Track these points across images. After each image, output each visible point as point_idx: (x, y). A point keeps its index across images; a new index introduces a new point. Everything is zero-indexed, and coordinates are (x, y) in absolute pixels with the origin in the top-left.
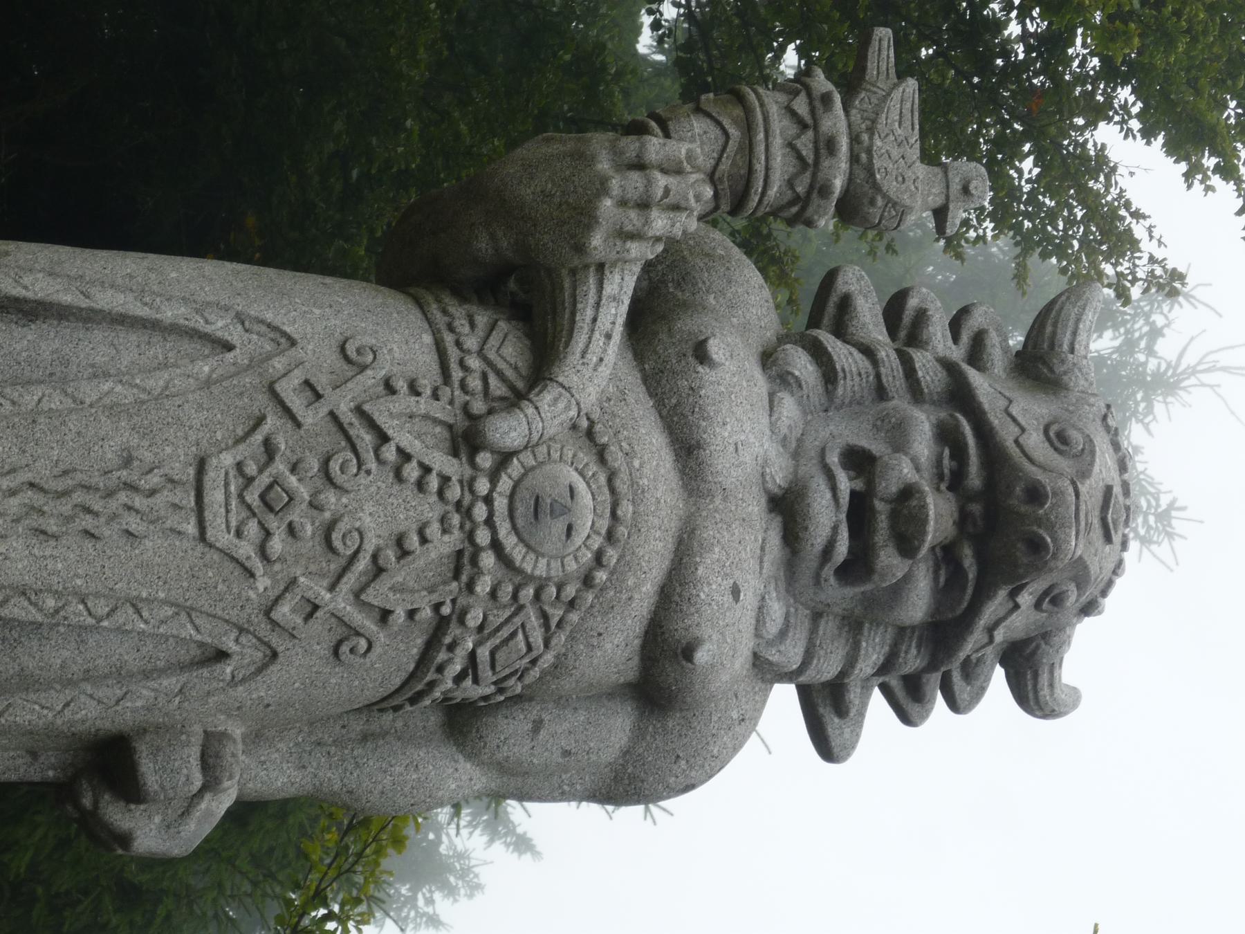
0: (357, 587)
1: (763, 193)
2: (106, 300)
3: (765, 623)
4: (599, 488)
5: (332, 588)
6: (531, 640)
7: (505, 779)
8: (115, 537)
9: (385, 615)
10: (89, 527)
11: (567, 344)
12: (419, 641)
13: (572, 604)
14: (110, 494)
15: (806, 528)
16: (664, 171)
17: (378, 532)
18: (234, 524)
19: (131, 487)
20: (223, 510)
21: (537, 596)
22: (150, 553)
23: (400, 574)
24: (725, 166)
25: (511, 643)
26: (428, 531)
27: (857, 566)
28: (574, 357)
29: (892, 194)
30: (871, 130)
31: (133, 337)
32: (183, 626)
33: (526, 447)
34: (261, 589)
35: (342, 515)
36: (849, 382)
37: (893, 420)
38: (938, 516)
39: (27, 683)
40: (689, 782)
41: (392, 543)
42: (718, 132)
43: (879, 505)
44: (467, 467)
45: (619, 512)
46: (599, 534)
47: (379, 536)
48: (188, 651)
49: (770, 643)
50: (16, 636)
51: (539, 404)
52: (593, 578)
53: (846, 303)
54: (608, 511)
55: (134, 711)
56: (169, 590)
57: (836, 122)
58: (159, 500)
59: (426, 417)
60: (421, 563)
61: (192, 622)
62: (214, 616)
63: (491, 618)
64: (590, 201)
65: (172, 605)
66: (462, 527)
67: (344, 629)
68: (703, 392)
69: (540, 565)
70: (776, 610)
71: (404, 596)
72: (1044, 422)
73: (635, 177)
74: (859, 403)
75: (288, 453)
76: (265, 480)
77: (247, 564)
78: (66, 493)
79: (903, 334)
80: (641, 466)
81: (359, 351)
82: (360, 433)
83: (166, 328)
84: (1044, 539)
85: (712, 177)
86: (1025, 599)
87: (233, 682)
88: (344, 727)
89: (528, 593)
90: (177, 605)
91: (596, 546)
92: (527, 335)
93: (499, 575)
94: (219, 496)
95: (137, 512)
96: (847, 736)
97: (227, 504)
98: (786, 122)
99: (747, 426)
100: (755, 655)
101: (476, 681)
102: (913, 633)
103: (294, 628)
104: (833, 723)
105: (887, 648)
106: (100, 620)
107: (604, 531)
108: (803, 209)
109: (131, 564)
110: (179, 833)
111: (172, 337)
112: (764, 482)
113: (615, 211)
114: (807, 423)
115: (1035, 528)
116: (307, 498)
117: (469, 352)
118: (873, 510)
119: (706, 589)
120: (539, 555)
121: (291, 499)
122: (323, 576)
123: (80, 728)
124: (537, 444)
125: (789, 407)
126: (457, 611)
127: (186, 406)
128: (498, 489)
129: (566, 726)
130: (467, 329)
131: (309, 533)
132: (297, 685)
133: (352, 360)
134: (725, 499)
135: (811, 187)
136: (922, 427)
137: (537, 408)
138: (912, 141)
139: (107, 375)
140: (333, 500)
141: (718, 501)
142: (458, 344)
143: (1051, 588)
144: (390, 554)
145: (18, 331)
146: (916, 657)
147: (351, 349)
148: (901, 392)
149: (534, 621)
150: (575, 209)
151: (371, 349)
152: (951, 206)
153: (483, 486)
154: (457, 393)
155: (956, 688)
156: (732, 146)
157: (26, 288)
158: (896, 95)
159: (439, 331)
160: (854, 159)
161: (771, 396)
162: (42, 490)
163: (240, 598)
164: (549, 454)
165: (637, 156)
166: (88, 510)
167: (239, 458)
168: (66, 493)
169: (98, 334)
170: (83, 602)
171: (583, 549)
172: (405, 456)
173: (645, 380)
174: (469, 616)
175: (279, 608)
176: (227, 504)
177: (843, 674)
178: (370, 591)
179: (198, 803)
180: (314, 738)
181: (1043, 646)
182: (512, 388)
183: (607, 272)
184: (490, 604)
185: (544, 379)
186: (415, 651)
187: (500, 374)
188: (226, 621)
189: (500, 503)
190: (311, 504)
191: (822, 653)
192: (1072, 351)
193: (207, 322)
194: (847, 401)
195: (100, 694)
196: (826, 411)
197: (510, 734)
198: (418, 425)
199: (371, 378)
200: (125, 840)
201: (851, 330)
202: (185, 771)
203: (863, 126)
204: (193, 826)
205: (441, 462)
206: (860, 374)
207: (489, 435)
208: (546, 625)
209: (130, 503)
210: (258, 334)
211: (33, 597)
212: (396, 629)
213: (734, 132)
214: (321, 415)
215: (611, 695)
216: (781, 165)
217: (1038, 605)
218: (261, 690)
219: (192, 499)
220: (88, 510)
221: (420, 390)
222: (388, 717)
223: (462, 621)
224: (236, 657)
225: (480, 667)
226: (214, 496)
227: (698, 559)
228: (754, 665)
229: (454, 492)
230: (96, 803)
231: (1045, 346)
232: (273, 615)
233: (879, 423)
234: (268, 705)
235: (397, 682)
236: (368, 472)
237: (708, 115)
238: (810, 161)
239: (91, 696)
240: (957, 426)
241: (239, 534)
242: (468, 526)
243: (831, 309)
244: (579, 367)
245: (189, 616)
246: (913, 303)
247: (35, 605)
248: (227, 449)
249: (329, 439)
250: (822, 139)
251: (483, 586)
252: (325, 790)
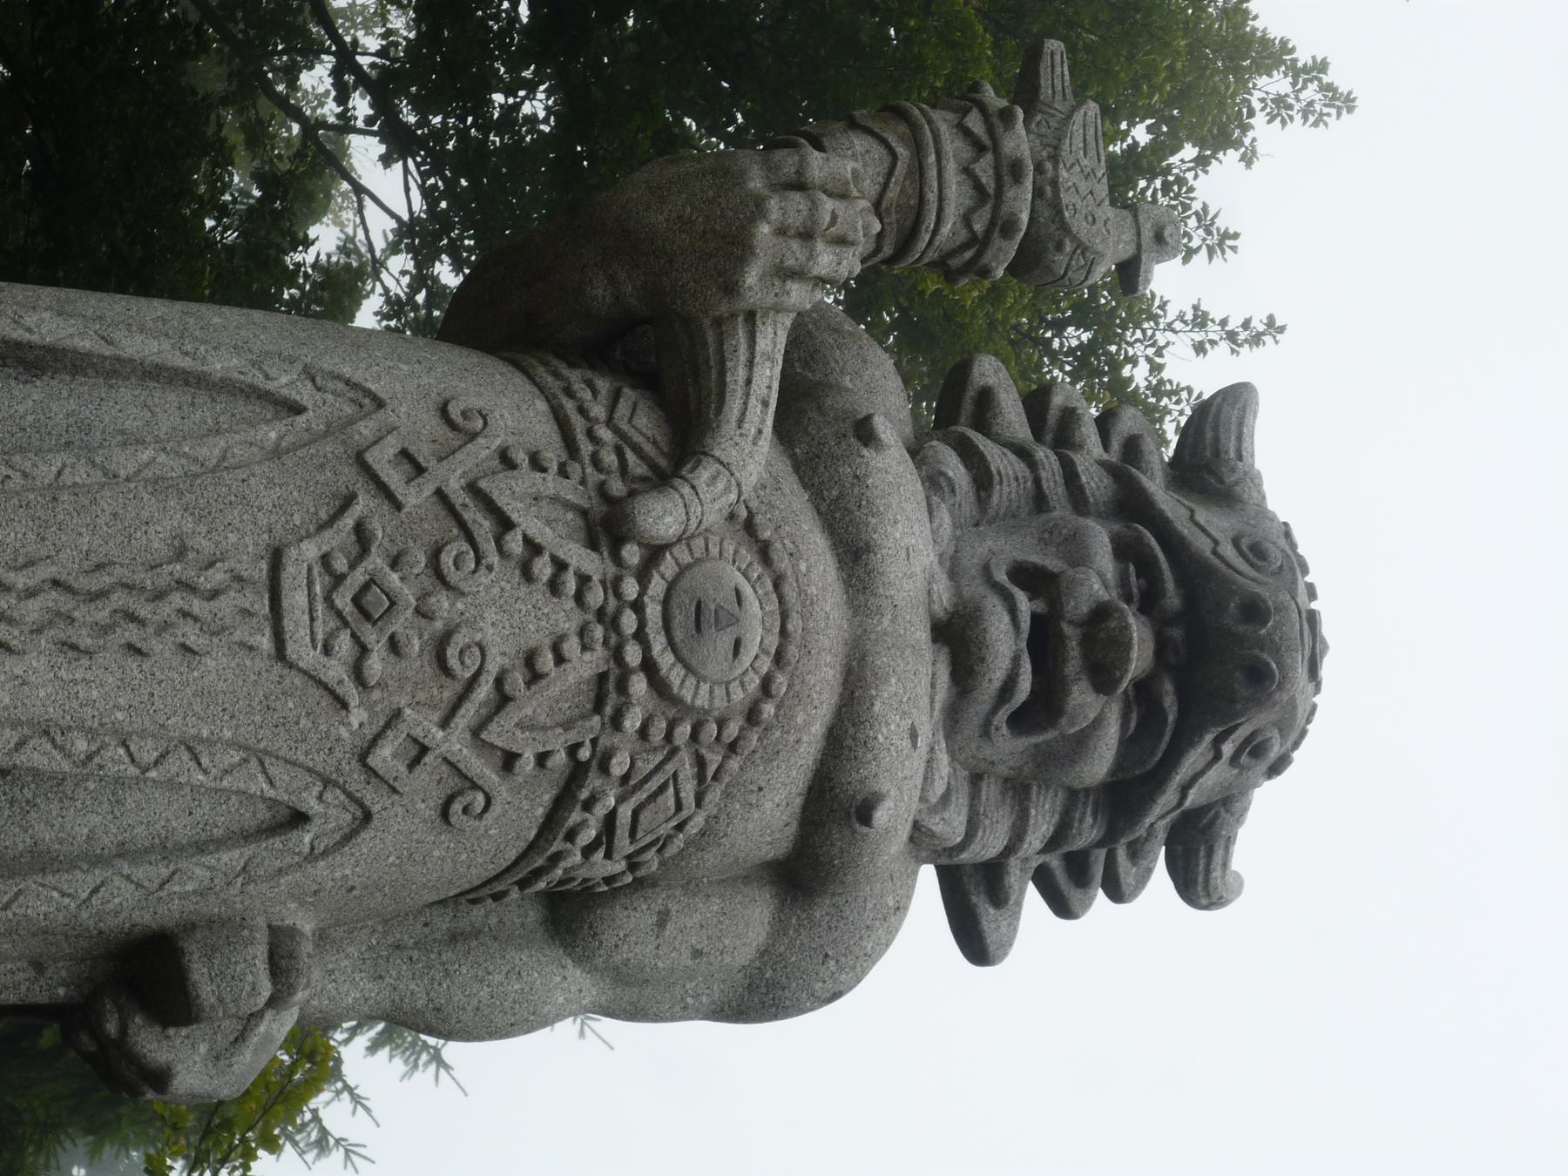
0: (474, 722)
1: (935, 232)
2: (135, 346)
3: (933, 781)
4: (766, 594)
5: (445, 723)
6: (683, 795)
7: (618, 990)
8: (168, 654)
9: (509, 761)
10: (135, 640)
11: (719, 410)
12: (547, 797)
13: (733, 748)
14: (159, 596)
15: (983, 660)
16: (830, 195)
17: (504, 648)
18: (320, 637)
19: (188, 587)
20: (306, 617)
21: (694, 737)
22: (213, 676)
23: (530, 705)
24: (892, 194)
25: (660, 799)
26: (565, 646)
27: (1042, 709)
28: (729, 427)
29: (1082, 236)
30: (1055, 159)
31: (172, 397)
32: (253, 777)
33: (679, 540)
34: (356, 725)
35: (458, 625)
36: (1006, 489)
37: (1065, 531)
38: (1140, 638)
39: (42, 862)
40: (837, 989)
41: (519, 663)
42: (883, 150)
43: (1068, 629)
44: (609, 562)
45: (790, 627)
46: (768, 653)
47: (504, 654)
48: (254, 813)
49: (933, 810)
50: (30, 796)
51: (695, 482)
52: (760, 712)
53: (986, 398)
54: (778, 623)
55: (184, 896)
56: (237, 726)
57: (1019, 141)
58: (225, 606)
59: (554, 499)
60: (555, 690)
61: (264, 772)
62: (294, 764)
63: (639, 764)
64: (744, 228)
65: (241, 747)
66: (605, 642)
67: (457, 780)
68: (870, 482)
69: (701, 692)
71: (534, 735)
72: (1231, 534)
73: (796, 196)
74: (1014, 516)
75: (386, 543)
76: (359, 577)
77: (340, 691)
78: (101, 595)
79: (1049, 437)
80: (808, 570)
81: (464, 414)
82: (477, 518)
83: (214, 385)
84: (1268, 664)
85: (877, 207)
86: (1228, 749)
87: (312, 856)
88: (426, 925)
89: (684, 730)
90: (247, 748)
91: (765, 670)
92: (659, 406)
93: (650, 707)
94: (301, 599)
95: (196, 619)
96: (1003, 929)
97: (311, 611)
98: (959, 143)
99: (916, 527)
100: (916, 826)
101: (608, 855)
102: (1087, 796)
103: (396, 779)
104: (988, 916)
105: (1057, 817)
106: (145, 770)
107: (773, 651)
108: (979, 254)
109: (188, 690)
110: (231, 1066)
111: (223, 397)
112: (931, 602)
113: (775, 240)
114: (958, 539)
115: (1257, 651)
116: (414, 603)
117: (597, 421)
118: (1061, 638)
119: (884, 730)
120: (700, 679)
121: (393, 603)
122: (434, 707)
123: (112, 922)
124: (692, 536)
126: (598, 755)
127: (253, 481)
128: (650, 592)
129: (697, 918)
130: (588, 395)
131: (417, 648)
132: (391, 859)
133: (457, 427)
134: (893, 621)
135: (992, 224)
136: (1100, 539)
137: (693, 487)
138: (1099, 175)
139: (141, 442)
140: (446, 605)
141: (886, 622)
142: (582, 411)
143: (1254, 734)
144: (518, 678)
145: (18, 390)
146: (1092, 827)
147: (455, 411)
148: (1063, 501)
149: (687, 770)
150: (724, 237)
151: (480, 413)
152: (1144, 258)
153: (631, 589)
154: (589, 470)
155: (1121, 869)
156: (901, 168)
157: (29, 330)
158: (1078, 117)
159: (555, 396)
160: (1038, 192)
161: (928, 498)
162: (70, 590)
163: (328, 737)
164: (707, 549)
165: (797, 172)
166: (132, 617)
167: (325, 548)
168: (101, 595)
170: (124, 744)
171: (751, 672)
172: (533, 548)
173: (797, 468)
174: (614, 761)
175: (378, 751)
176: (311, 611)
177: (1009, 850)
178: (493, 727)
179: (256, 1026)
180: (390, 940)
181: (1223, 814)
182: (653, 466)
183: (759, 323)
184: (638, 746)
185: (695, 453)
186: (540, 811)
187: (637, 449)
188: (309, 770)
189: (653, 611)
190: (417, 611)
191: (987, 822)
192: (1240, 457)
193: (267, 377)
194: (1002, 512)
195: (139, 874)
196: (977, 525)
197: (630, 929)
198: (546, 508)
199: (483, 450)
200: (160, 1078)
201: (995, 429)
202: (250, 978)
203: (1044, 153)
204: (248, 1056)
205: (580, 557)
206: (1017, 479)
207: (640, 519)
208: (701, 777)
209: (186, 607)
210: (334, 393)
211: (58, 738)
212: (520, 779)
213: (903, 152)
214: (427, 493)
215: (746, 879)
216: (957, 193)
217: (1234, 760)
218: (346, 867)
219: (267, 602)
220: (132, 617)
221: (545, 464)
222: (478, 912)
223: (604, 769)
224: (317, 821)
225: (619, 832)
226: (295, 600)
227: (873, 692)
228: (911, 839)
229: (596, 597)
230: (123, 1030)
231: (1208, 453)
232: (371, 761)
233: (1046, 535)
234: (352, 888)
235: (512, 854)
236: (490, 568)
237: (869, 131)
238: (991, 191)
239: (128, 878)
240: (1139, 539)
241: (327, 650)
242: (613, 640)
243: (968, 406)
244: (737, 439)
245: (261, 763)
246: (1057, 400)
247: (62, 749)
248: (308, 536)
249: (436, 525)
250: (1004, 162)
251: (632, 722)
252: (407, 1007)
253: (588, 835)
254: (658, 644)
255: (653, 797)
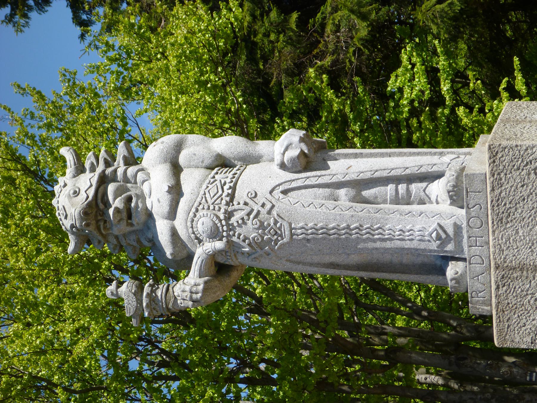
13: (200, 204)
21: (209, 207)
70: (145, 188)
89: (212, 207)
94: (286, 233)
101: (221, 181)
108: (152, 289)
129: (195, 161)
144: (246, 218)
145: (335, 261)
149: (209, 199)
169: (316, 261)
208: (205, 198)
251: (222, 210)
253: (226, 187)
254: (219, 225)
255: (215, 195)
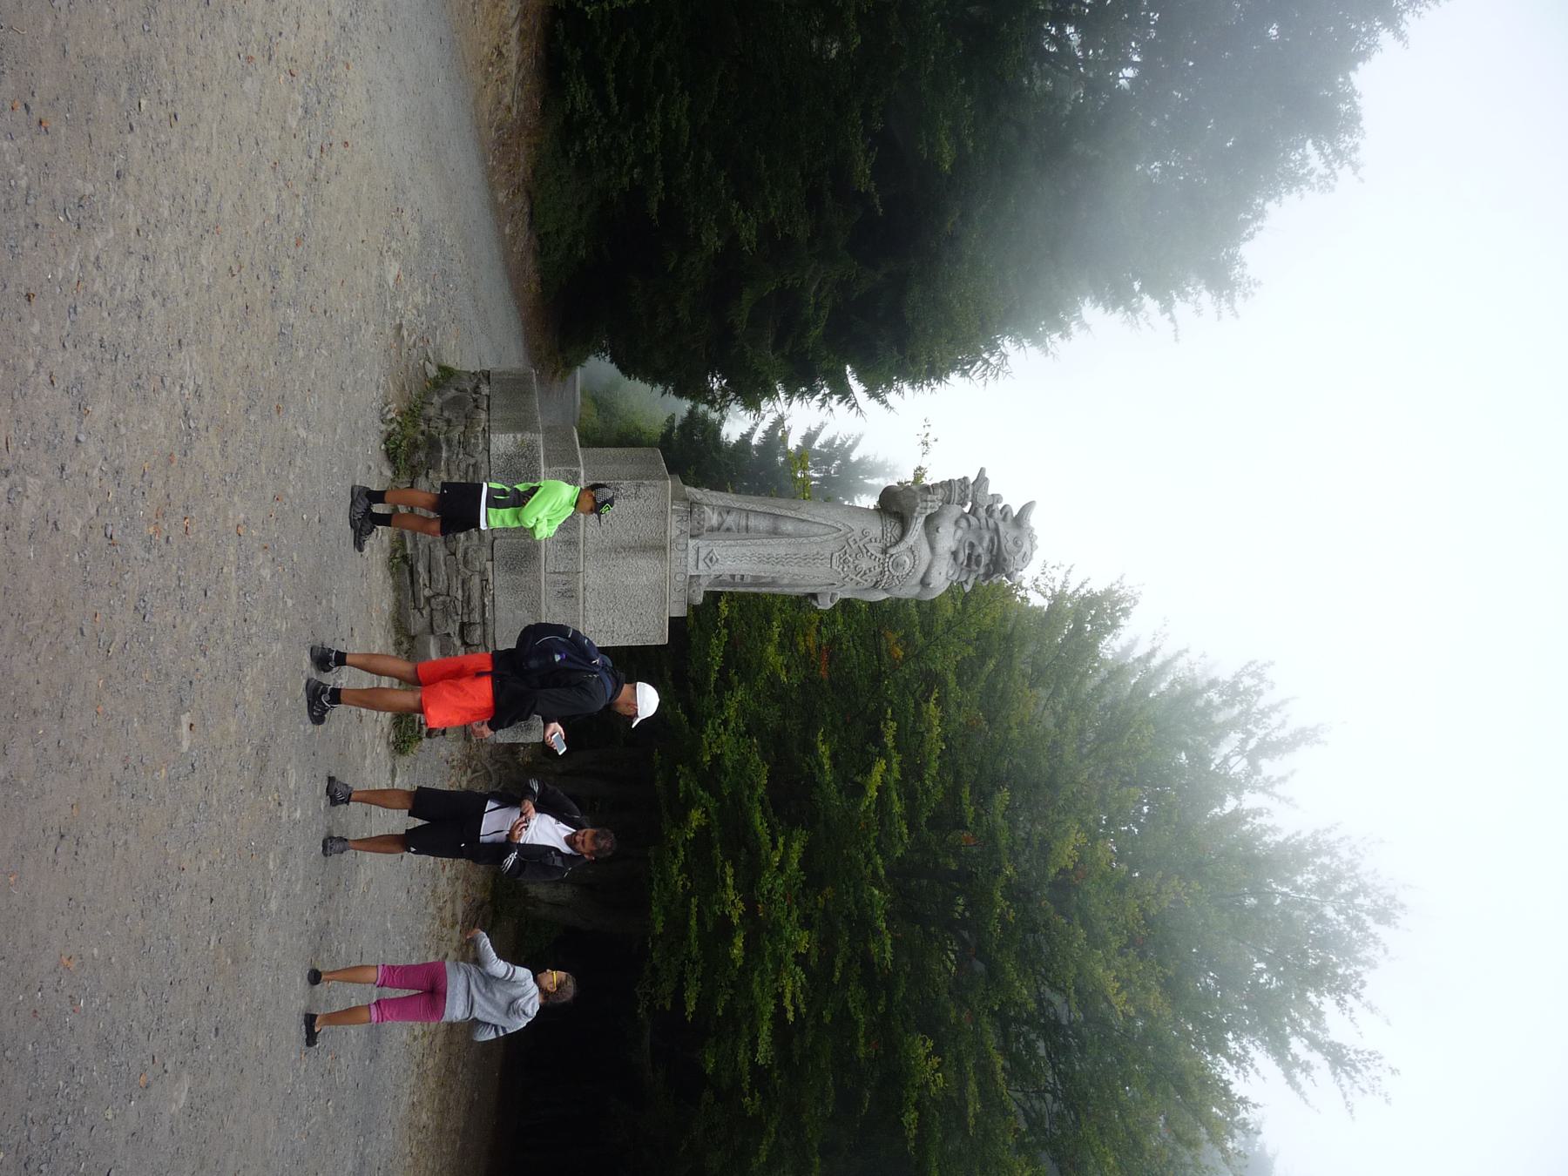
125: (959, 533)
133: (864, 534)
